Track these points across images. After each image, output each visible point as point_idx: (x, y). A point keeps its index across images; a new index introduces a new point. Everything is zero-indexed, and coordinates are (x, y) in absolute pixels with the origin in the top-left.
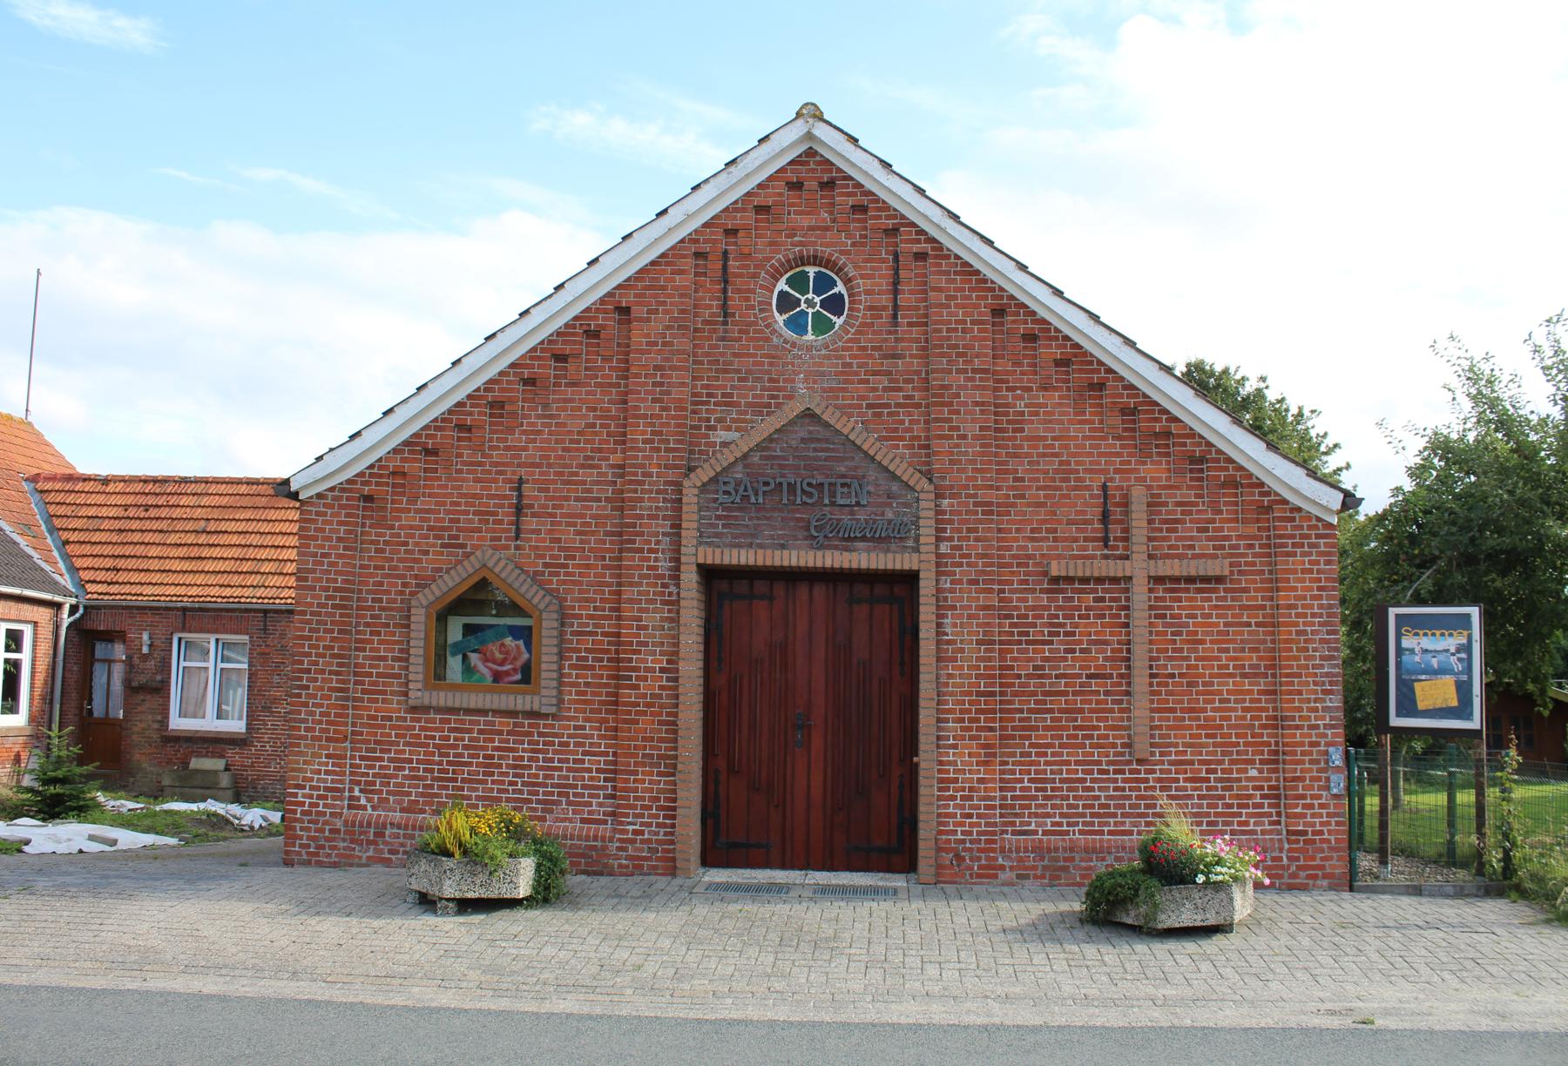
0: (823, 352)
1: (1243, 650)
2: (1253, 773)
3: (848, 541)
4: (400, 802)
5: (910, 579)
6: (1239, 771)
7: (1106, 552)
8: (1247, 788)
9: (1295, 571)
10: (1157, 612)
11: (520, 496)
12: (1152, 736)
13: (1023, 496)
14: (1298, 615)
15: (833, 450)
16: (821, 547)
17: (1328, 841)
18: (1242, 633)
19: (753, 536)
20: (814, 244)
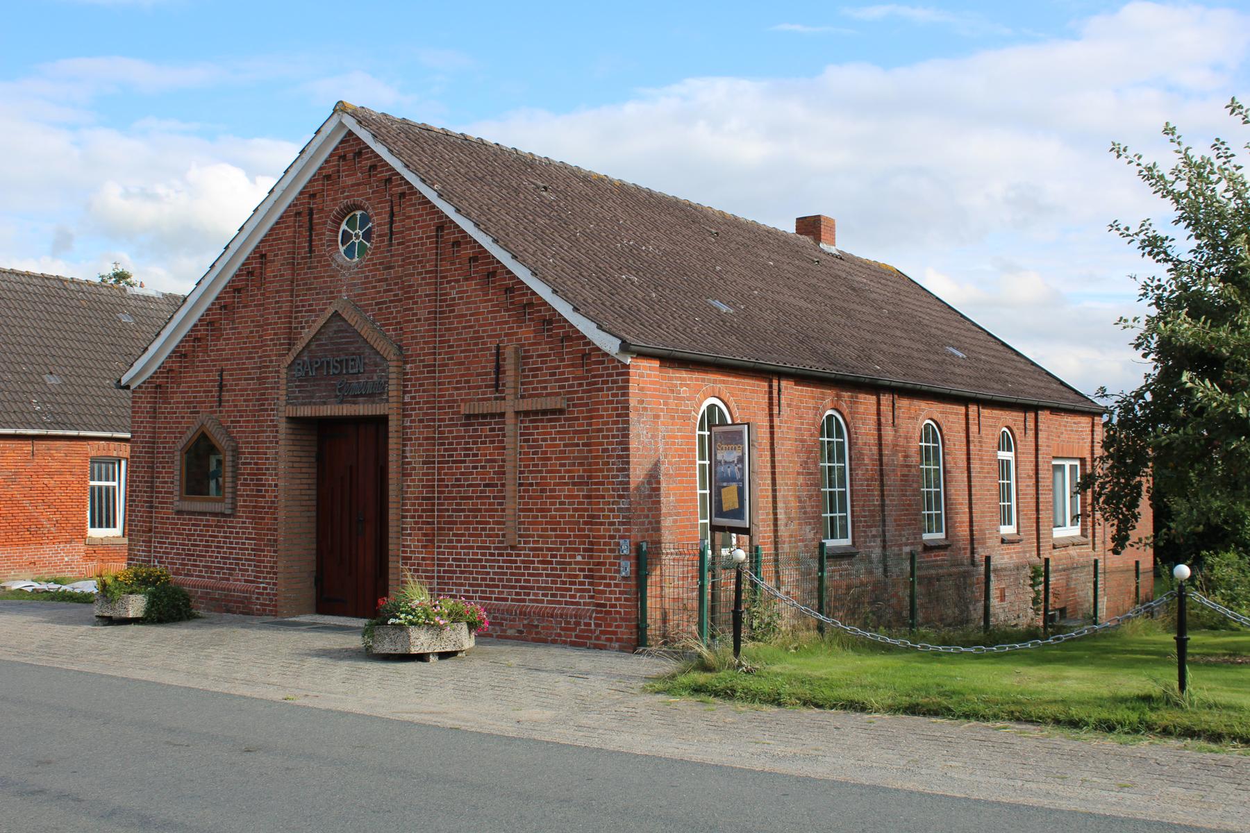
0: (356, 270)
1: (574, 465)
2: (579, 558)
3: (354, 398)
4: (172, 568)
5: (383, 420)
6: (571, 557)
7: (497, 395)
8: (574, 570)
9: (602, 403)
10: (525, 436)
11: (222, 380)
12: (520, 529)
13: (452, 359)
14: (604, 437)
15: (348, 337)
16: (342, 402)
17: (619, 613)
18: (573, 452)
19: (312, 397)
20: (353, 196)
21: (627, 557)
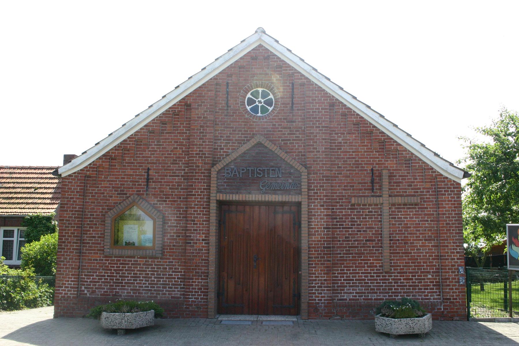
0: (265, 120)
1: (425, 230)
2: (430, 276)
3: (275, 191)
6: (424, 276)
7: (373, 194)
8: (427, 282)
9: (445, 201)
11: (148, 175)
13: (341, 174)
17: (459, 302)
20: (262, 80)
21: (462, 275)
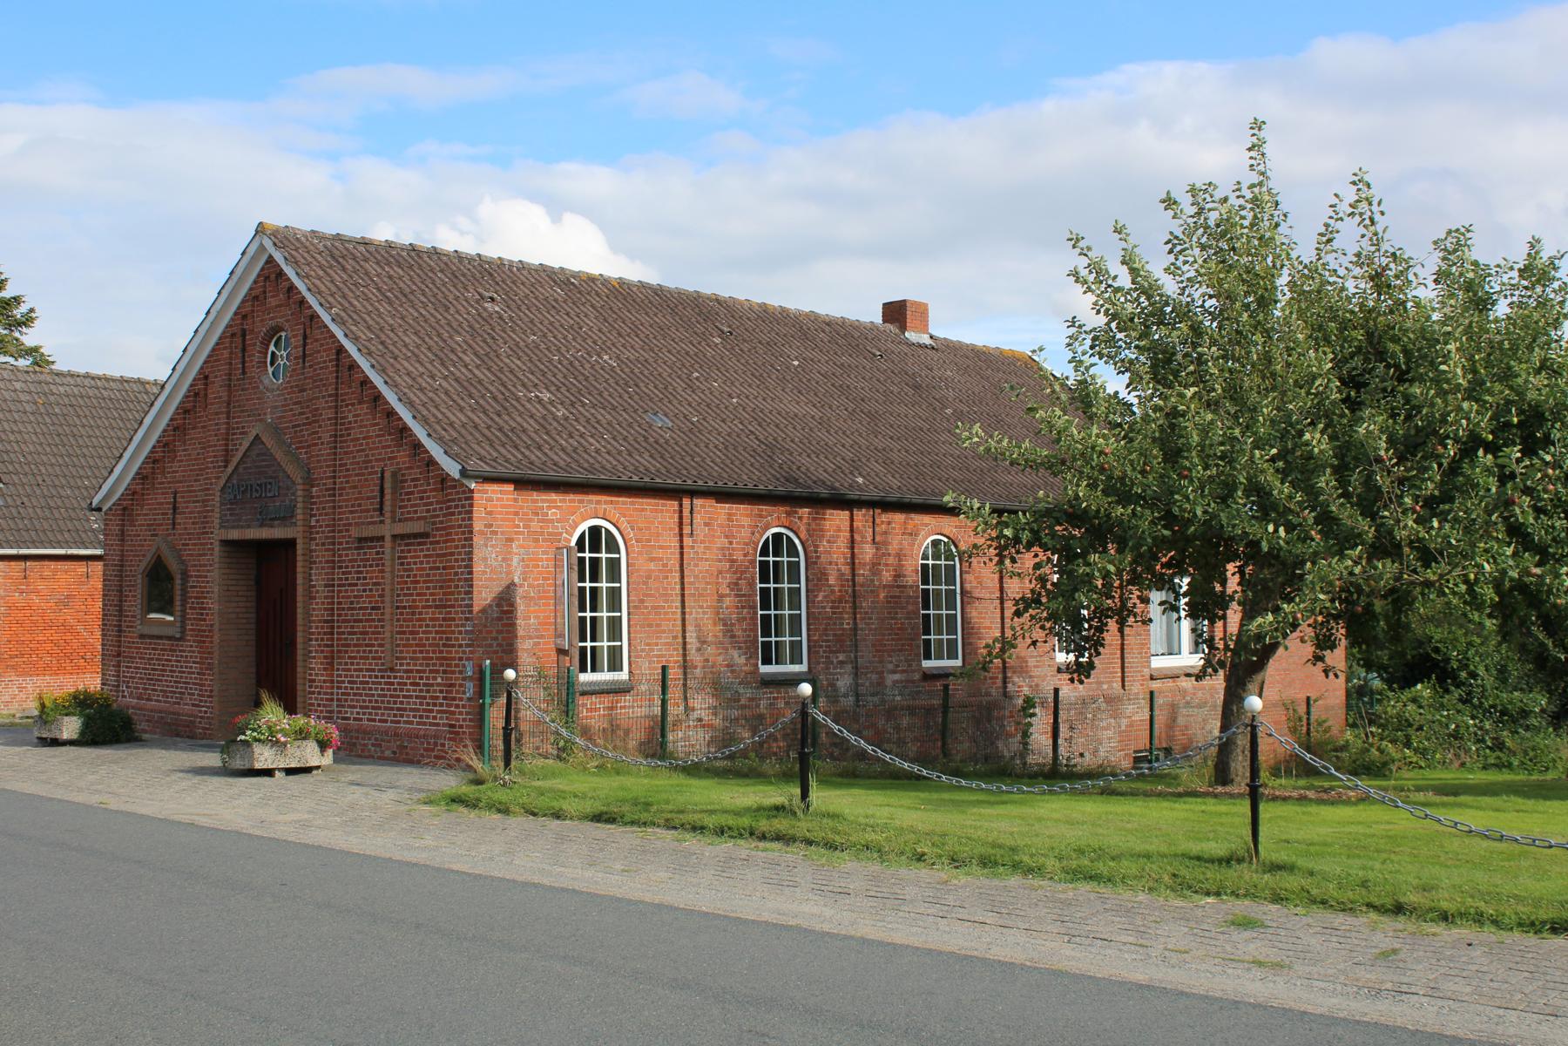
2: (439, 680)
5: (291, 543)
16: (262, 525)
21: (471, 678)
